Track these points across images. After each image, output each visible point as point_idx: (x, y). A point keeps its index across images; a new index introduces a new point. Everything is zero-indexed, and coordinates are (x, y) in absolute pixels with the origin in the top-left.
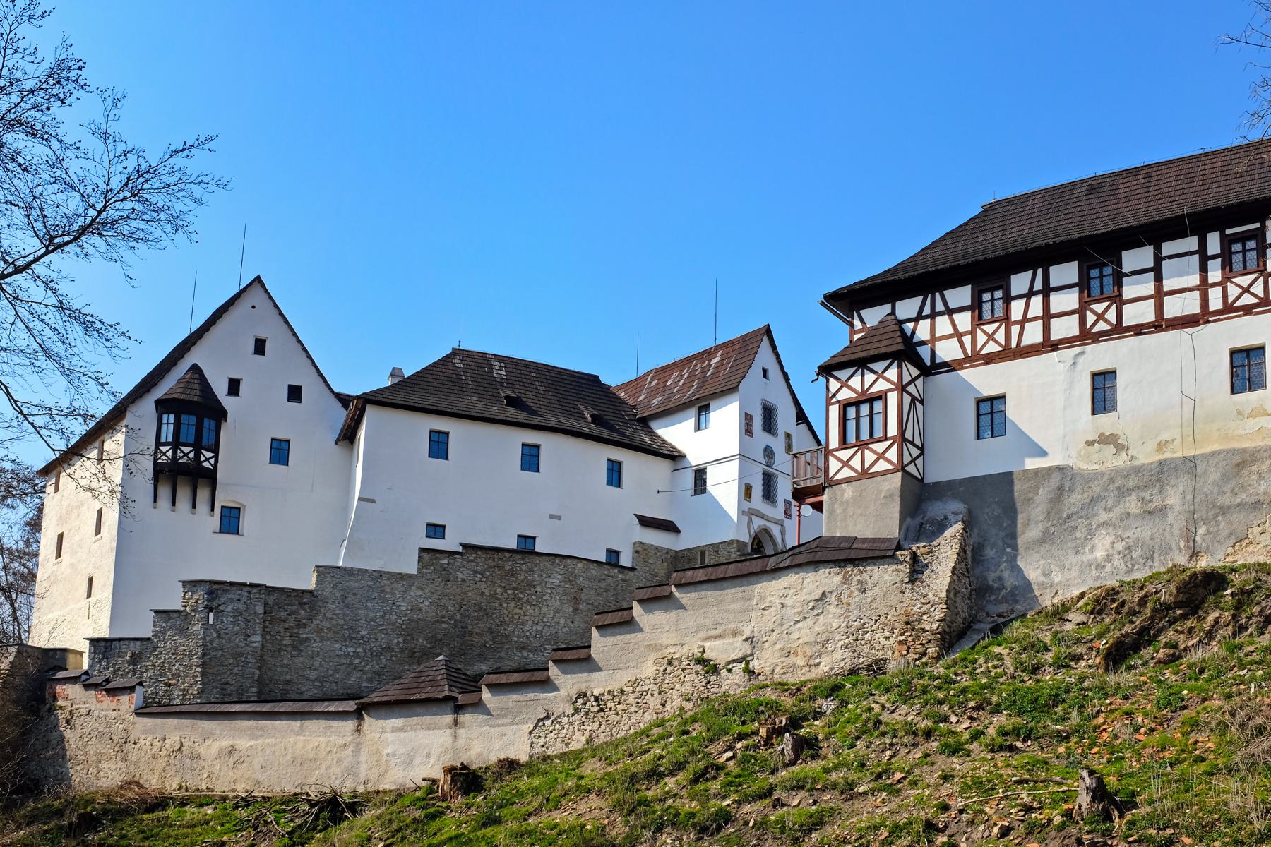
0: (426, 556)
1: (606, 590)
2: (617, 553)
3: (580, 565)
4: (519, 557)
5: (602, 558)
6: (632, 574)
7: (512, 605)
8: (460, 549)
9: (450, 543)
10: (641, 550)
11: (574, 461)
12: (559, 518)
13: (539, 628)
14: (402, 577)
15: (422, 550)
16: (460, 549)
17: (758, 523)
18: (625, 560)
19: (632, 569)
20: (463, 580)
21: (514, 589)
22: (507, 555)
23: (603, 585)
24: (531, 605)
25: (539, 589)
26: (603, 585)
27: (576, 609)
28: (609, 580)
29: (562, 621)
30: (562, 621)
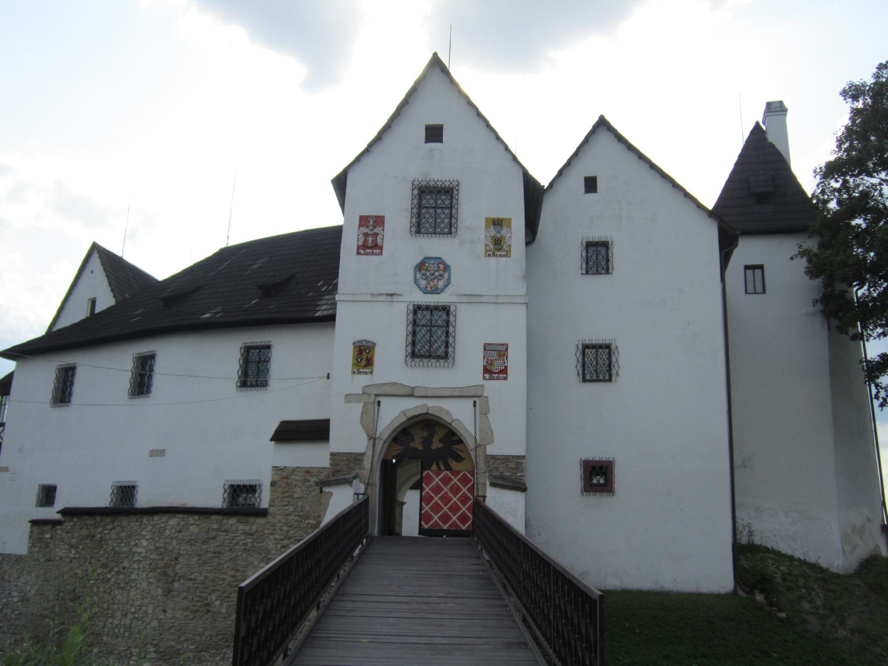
0: (36, 530)
1: (218, 554)
2: (251, 489)
3: (173, 522)
4: (109, 519)
5: (216, 500)
6: (260, 521)
7: (101, 589)
8: (59, 517)
9: (51, 513)
10: (283, 478)
11: (198, 366)
12: (161, 453)
13: (128, 622)
14: (19, 559)
15: (35, 523)
16: (59, 517)
17: (393, 412)
18: (264, 500)
19: (263, 513)
20: (61, 559)
21: (104, 566)
22: (98, 518)
23: (212, 547)
24: (119, 588)
25: (126, 564)
26: (212, 547)
27: (168, 592)
28: (222, 537)
29: (150, 611)
30: (150, 611)
